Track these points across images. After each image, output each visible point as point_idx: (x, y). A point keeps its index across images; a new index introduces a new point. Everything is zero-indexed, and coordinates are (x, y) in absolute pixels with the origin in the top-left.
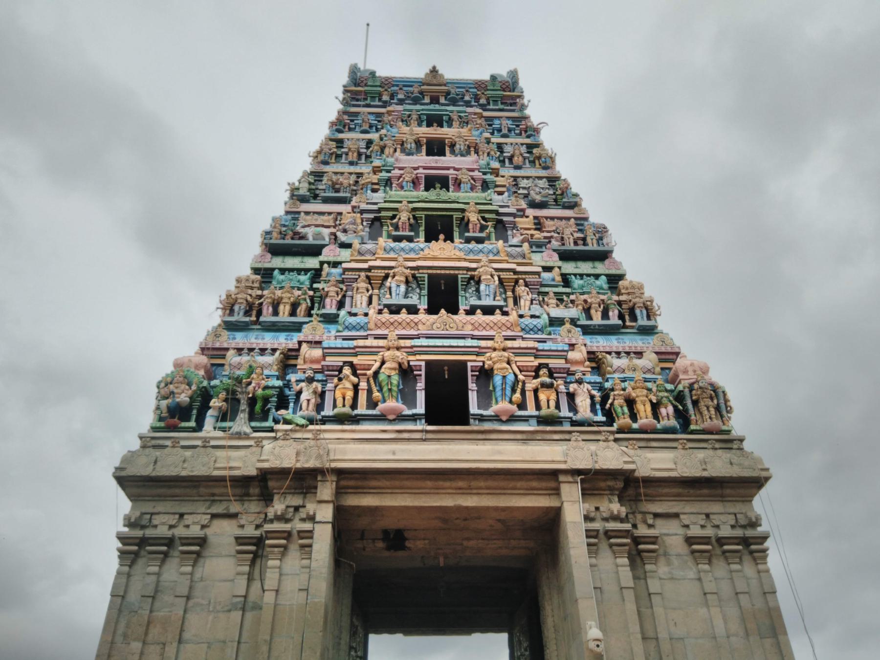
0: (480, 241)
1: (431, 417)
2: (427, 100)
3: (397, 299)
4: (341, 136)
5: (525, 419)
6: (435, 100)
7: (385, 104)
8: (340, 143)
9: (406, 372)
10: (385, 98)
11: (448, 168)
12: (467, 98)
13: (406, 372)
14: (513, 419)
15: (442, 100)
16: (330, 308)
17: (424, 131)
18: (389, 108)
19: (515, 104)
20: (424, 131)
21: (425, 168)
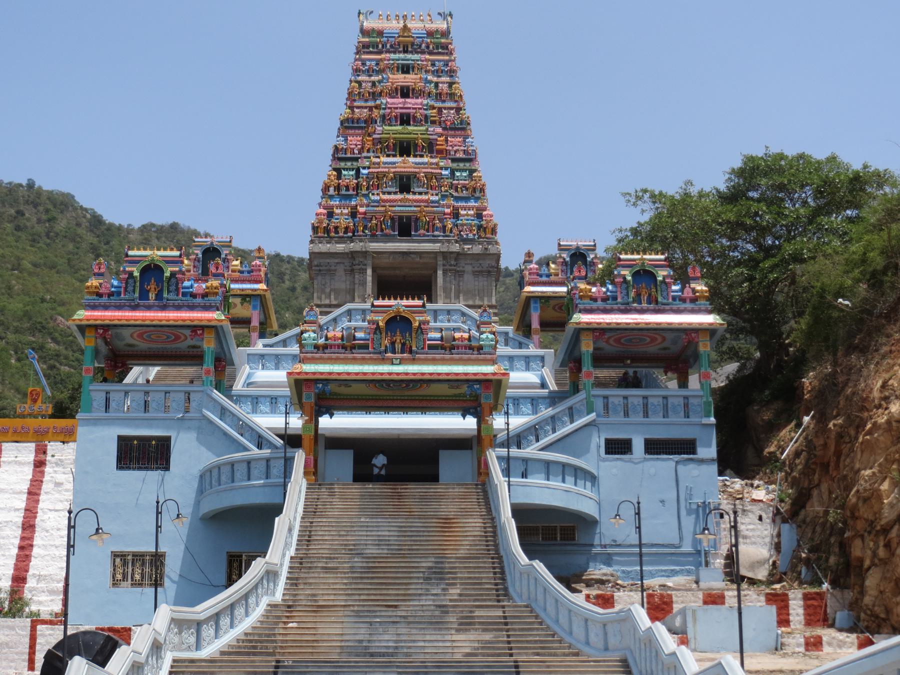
0: (422, 156)
1: (400, 235)
2: (401, 49)
3: (389, 189)
4: (360, 78)
5: (428, 236)
6: (405, 51)
7: (380, 53)
8: (360, 83)
9: (392, 219)
10: (380, 46)
11: (409, 108)
12: (423, 46)
13: (392, 219)
14: (424, 235)
15: (410, 49)
16: (364, 192)
17: (401, 79)
18: (383, 56)
19: (447, 48)
20: (401, 79)
21: (401, 108)
